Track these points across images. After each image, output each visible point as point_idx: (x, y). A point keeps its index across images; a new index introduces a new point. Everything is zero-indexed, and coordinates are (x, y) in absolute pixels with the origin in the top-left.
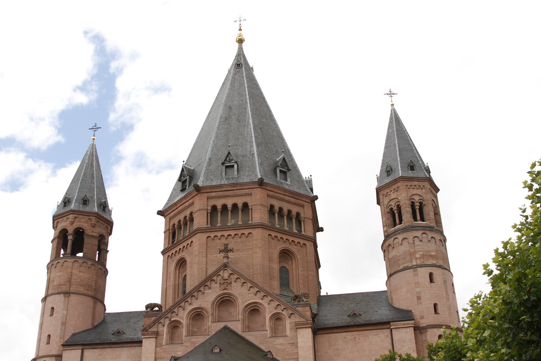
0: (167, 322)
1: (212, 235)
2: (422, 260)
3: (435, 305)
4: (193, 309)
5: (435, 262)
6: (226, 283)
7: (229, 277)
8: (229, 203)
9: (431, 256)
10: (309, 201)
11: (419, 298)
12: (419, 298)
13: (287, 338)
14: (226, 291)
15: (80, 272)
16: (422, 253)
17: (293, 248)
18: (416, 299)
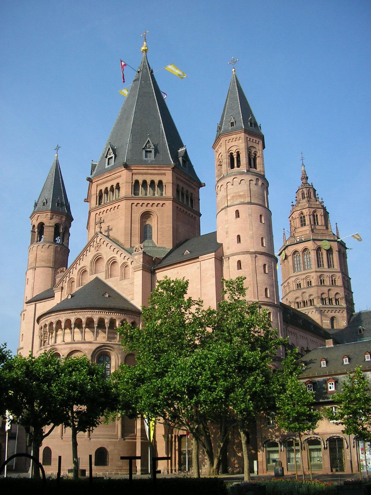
0: (68, 279)
1: (98, 212)
2: (232, 201)
3: (239, 237)
4: (81, 268)
5: (242, 200)
6: (99, 246)
7: (100, 241)
8: (109, 185)
9: (240, 196)
10: (170, 169)
11: (227, 233)
12: (227, 233)
13: (129, 279)
14: (98, 252)
15: (42, 252)
16: (232, 195)
17: (154, 209)
18: (225, 234)
